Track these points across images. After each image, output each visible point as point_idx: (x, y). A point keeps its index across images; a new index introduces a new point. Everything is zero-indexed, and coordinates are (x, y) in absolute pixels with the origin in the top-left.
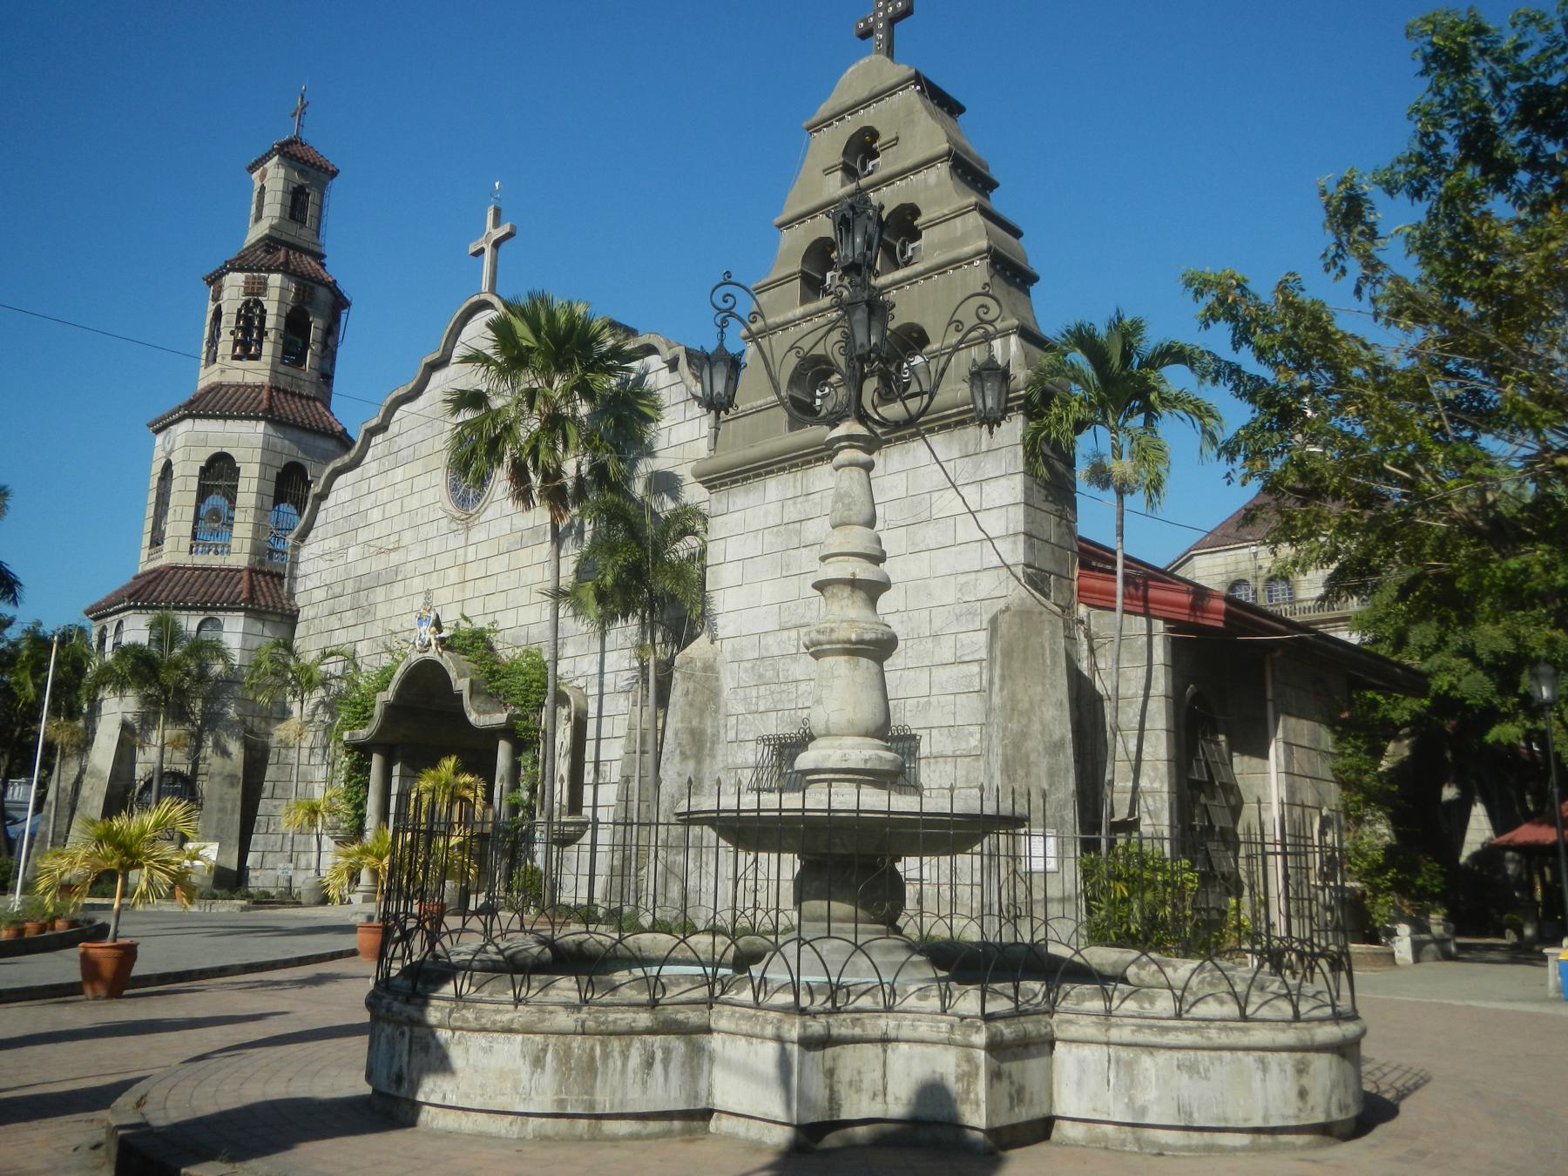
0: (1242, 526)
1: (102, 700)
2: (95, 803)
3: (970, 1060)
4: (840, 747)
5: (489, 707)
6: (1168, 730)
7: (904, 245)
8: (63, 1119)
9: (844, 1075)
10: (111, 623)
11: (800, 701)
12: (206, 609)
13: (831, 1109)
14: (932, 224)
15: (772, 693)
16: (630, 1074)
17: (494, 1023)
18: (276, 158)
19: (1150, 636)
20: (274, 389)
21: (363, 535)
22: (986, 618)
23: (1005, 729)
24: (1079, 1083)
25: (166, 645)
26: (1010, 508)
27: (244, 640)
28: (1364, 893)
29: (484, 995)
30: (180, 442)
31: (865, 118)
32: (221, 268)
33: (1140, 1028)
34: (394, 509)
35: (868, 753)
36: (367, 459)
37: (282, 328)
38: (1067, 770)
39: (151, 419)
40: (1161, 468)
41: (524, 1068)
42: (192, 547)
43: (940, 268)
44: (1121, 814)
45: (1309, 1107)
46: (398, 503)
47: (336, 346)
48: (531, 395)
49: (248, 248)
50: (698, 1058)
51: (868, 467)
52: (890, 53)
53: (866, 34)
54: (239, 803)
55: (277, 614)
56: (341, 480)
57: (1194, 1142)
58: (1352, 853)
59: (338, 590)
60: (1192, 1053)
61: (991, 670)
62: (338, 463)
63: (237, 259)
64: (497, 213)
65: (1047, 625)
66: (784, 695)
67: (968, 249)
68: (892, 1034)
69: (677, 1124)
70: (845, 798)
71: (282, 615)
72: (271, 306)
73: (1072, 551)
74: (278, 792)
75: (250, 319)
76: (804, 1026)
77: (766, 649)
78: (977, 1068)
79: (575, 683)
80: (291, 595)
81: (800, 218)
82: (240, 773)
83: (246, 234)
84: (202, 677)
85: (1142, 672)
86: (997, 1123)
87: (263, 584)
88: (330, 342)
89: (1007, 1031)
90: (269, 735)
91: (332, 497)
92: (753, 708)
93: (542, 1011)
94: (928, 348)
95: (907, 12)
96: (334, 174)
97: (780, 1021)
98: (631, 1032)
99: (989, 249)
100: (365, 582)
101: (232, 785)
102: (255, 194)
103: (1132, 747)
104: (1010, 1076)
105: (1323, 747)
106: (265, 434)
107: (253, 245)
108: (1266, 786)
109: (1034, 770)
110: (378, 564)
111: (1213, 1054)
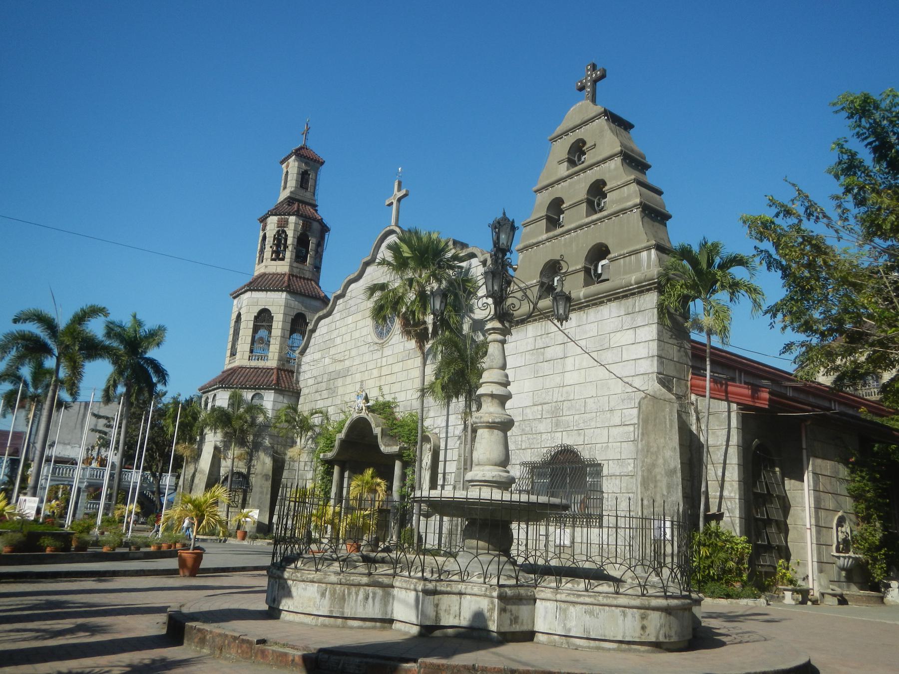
0: (783, 353)
1: (206, 434)
2: (201, 488)
3: (492, 603)
4: (483, 470)
5: (391, 443)
6: (738, 464)
7: (599, 200)
8: (156, 615)
9: (443, 607)
10: (210, 395)
11: (543, 443)
12: (255, 389)
13: (436, 620)
14: (612, 190)
15: (528, 439)
16: (359, 602)
17: (307, 578)
18: (294, 157)
19: (729, 412)
20: (291, 275)
21: (332, 351)
22: (637, 401)
23: (643, 462)
24: (545, 618)
25: (236, 407)
26: (650, 342)
27: (274, 405)
28: (867, 562)
29: (306, 568)
30: (245, 303)
31: (579, 134)
32: (266, 214)
33: (569, 594)
34: (347, 338)
35: (494, 473)
36: (335, 312)
37: (295, 244)
38: (678, 485)
39: (231, 292)
40: (726, 323)
41: (318, 596)
42: (250, 357)
43: (616, 214)
44: (713, 510)
45: (647, 633)
46: (350, 334)
47: (323, 251)
48: (411, 281)
49: (279, 203)
50: (387, 598)
51: (503, 342)
52: (594, 100)
53: (582, 89)
54: (270, 489)
55: (290, 391)
56: (322, 322)
57: (591, 645)
58: (859, 538)
59: (320, 380)
60: (591, 606)
61: (638, 430)
62: (321, 313)
63: (274, 210)
64: (400, 184)
65: (668, 406)
66: (535, 440)
67: (630, 204)
68: (463, 591)
69: (378, 624)
70: (486, 494)
71: (293, 392)
72: (290, 233)
73: (688, 365)
75: (280, 239)
76: (425, 585)
77: (526, 416)
78: (495, 606)
79: (434, 431)
80: (298, 381)
81: (545, 187)
82: (270, 474)
83: (279, 196)
84: (253, 424)
85: (725, 432)
86: (503, 630)
87: (284, 376)
88: (319, 250)
89: (509, 592)
90: (285, 454)
91: (318, 331)
92: (519, 447)
93: (325, 574)
94: (609, 256)
95: (603, 76)
96: (322, 163)
97: (416, 583)
98: (359, 585)
99: (641, 203)
100: (333, 376)
101: (267, 480)
102: (284, 175)
103: (720, 473)
104: (511, 611)
105: (841, 476)
106: (286, 298)
107: (282, 202)
108: (803, 498)
109: (659, 484)
110: (339, 367)
111: (601, 607)
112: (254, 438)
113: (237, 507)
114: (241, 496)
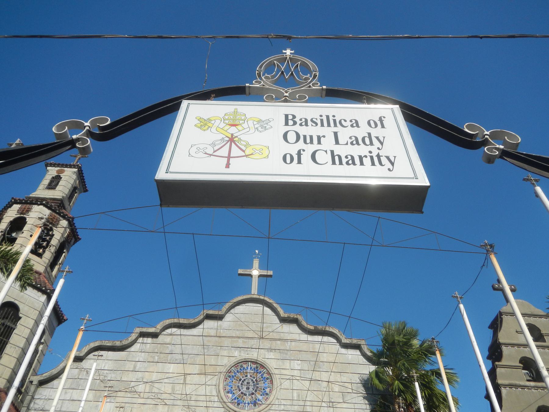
18: (76, 170)
36: (132, 349)
37: (57, 248)
83: (34, 191)
96: (86, 191)
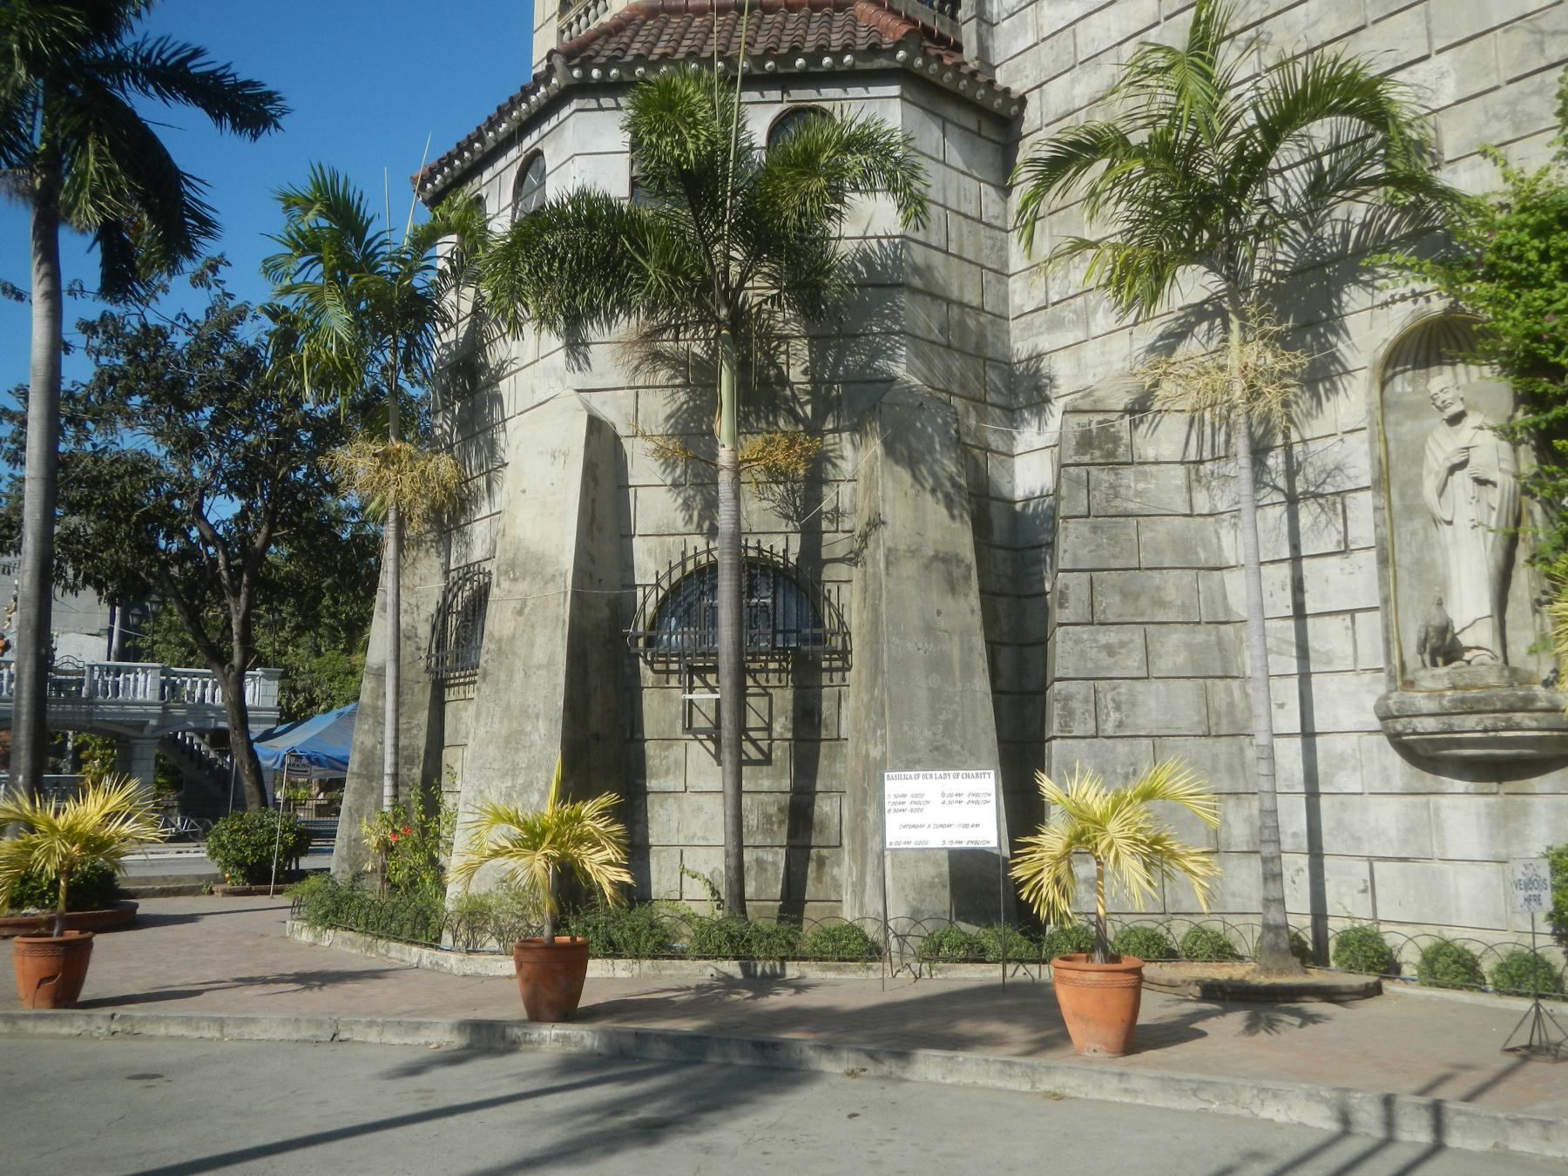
2: (540, 656)
12: (784, 81)
54: (979, 643)
74: (1111, 604)
101: (953, 588)
112: (817, 360)
113: (767, 760)
114: (784, 698)
